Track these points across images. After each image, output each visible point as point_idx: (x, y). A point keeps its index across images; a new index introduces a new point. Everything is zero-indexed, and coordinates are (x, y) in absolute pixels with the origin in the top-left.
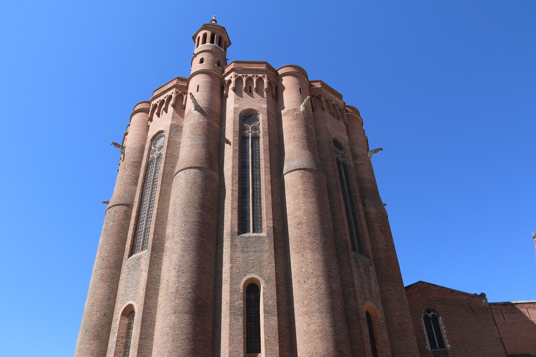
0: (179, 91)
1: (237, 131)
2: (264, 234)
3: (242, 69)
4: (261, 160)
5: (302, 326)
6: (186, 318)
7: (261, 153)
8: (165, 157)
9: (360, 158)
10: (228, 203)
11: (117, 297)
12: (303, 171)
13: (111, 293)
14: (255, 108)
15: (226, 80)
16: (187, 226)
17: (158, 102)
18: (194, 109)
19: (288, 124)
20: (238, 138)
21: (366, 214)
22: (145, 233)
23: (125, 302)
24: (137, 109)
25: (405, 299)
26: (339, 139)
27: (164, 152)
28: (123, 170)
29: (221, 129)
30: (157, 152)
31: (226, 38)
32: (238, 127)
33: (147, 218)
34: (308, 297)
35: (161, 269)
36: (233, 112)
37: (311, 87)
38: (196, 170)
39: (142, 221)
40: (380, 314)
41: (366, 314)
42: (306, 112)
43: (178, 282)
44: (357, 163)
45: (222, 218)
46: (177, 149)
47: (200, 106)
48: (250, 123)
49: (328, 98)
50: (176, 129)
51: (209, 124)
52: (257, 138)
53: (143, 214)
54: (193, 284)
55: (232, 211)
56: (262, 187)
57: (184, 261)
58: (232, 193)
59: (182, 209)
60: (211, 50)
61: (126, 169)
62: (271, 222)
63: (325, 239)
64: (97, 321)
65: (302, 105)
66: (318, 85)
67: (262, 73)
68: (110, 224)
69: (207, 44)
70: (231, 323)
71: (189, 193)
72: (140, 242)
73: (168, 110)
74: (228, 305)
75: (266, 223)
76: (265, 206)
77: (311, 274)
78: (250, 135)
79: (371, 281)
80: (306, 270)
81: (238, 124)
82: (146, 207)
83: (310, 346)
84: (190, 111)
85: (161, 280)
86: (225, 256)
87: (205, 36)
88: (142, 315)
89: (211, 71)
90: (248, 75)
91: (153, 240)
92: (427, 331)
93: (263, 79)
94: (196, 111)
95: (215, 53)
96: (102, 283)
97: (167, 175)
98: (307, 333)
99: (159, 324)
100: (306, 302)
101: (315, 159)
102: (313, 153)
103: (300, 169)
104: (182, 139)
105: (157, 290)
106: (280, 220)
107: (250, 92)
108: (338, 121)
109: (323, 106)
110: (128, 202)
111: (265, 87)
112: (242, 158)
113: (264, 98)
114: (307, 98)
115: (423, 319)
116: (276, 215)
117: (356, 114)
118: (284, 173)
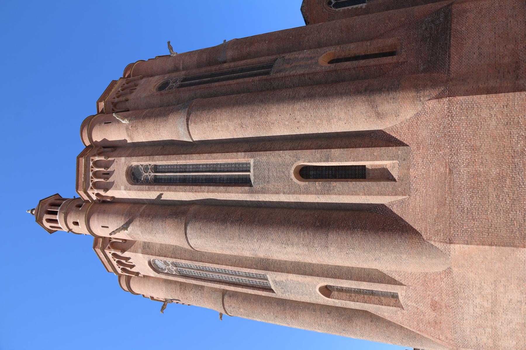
0: (108, 246)
1: (148, 188)
2: (252, 161)
3: (84, 182)
4: (178, 164)
5: (341, 125)
6: (333, 236)
7: (171, 164)
8: (175, 259)
9: (177, 64)
10: (220, 196)
11: (312, 302)
12: (189, 122)
13: (308, 309)
14: (125, 169)
15: (96, 199)
16: (243, 236)
17: (119, 267)
18: (126, 231)
19: (142, 136)
20: (155, 186)
21: (233, 60)
22: (250, 277)
23: (317, 295)
24: (127, 288)
25: (318, 25)
26: (158, 85)
27: (170, 260)
28: (189, 300)
29: (146, 204)
30: (170, 267)
31: (51, 198)
32: (144, 186)
33: (236, 275)
34: (314, 120)
35: (286, 261)
36: (129, 191)
37: (104, 112)
38: (188, 228)
39: (239, 280)
40: (331, 50)
41: (331, 64)
42: (130, 118)
43: (297, 244)
44: (182, 68)
45: (235, 202)
46: (167, 247)
47: (123, 225)
48: (141, 174)
49: (115, 95)
50: (147, 248)
51: (142, 216)
52: (156, 167)
53: (232, 279)
54: (300, 230)
55: (228, 192)
56: (204, 163)
57: (277, 239)
58: (211, 192)
59: (227, 242)
60: (65, 214)
61: (187, 297)
62: (239, 154)
63: (257, 101)
64: (335, 321)
65: (122, 122)
66: (102, 105)
67: (89, 162)
68: (242, 311)
69: (58, 218)
70: (337, 193)
71: (211, 235)
72: (259, 282)
73: (128, 257)
74: (320, 196)
75: (241, 159)
76: (224, 160)
77: (291, 116)
78: (152, 174)
79: (299, 57)
80: (287, 121)
81: (141, 187)
82: (225, 277)
83: (360, 119)
84: (128, 234)
85: (296, 261)
86: (272, 199)
87: (49, 221)
88: (330, 278)
89: (87, 214)
90: (90, 176)
91: (257, 269)
92: (349, 6)
93: (95, 160)
94: (128, 229)
95: (67, 210)
96: (300, 317)
97: (193, 257)
98: (347, 121)
99: (338, 262)
100: (318, 121)
101: (178, 110)
102: (171, 111)
103: (188, 124)
104: (157, 242)
105: (305, 265)
106: (238, 145)
107: (108, 174)
108: (139, 85)
109: (124, 100)
110: (220, 295)
111: (104, 159)
112: (176, 182)
113: (115, 160)
114: (115, 116)
115: (336, 9)
116: (233, 149)
117: (133, 67)
118: (191, 141)
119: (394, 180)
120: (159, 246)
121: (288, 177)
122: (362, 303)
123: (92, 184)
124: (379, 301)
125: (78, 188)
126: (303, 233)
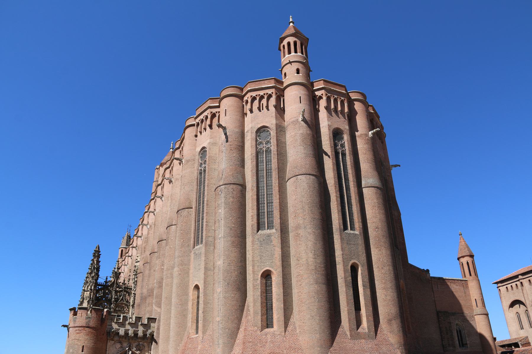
5: (382, 296)
6: (324, 287)
13: (242, 257)
30: (264, 145)
38: (314, 177)
62: (361, 224)
73: (269, 108)
78: (340, 151)
81: (332, 140)
100: (384, 281)
103: (375, 187)
110: (241, 182)
113: (346, 119)
119: (357, 330)
120: (283, 140)
121: (351, 259)
122: (260, 301)
123: (329, 96)
124: (263, 314)
125: (325, 82)
126: (323, 267)
